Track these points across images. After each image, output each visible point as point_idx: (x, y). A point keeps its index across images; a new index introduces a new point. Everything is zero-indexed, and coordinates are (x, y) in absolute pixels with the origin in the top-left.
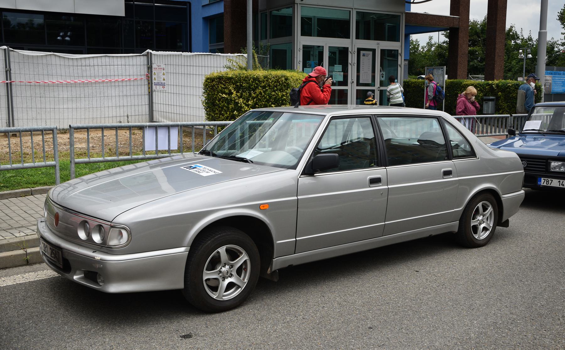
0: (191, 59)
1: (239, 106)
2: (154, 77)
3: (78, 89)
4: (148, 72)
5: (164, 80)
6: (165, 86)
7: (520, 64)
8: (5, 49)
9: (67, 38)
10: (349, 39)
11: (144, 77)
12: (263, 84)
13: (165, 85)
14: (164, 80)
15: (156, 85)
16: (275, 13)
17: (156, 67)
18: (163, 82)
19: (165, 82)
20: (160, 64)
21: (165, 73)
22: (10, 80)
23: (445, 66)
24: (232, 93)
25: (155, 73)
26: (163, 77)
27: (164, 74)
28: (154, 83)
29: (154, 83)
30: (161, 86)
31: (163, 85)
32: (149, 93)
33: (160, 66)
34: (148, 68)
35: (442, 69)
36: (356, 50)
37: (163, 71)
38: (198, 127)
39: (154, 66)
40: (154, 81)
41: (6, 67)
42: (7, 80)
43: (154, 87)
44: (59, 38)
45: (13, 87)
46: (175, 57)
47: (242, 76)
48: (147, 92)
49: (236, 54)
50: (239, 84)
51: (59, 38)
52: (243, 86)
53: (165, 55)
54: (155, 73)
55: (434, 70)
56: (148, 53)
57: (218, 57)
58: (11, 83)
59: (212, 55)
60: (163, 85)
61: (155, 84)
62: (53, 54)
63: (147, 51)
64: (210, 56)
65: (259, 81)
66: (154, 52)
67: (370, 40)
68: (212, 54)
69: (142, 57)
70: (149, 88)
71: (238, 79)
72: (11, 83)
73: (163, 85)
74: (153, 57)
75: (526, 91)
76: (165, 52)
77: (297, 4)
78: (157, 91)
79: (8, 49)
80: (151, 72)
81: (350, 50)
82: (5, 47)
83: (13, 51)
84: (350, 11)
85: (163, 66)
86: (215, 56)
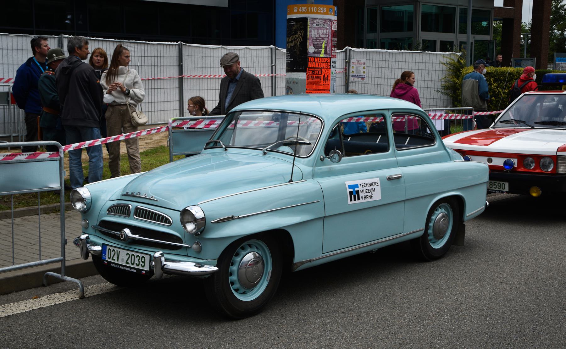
0: (384, 55)
1: (496, 94)
2: (351, 70)
3: (206, 80)
4: (346, 66)
5: (364, 72)
6: (365, 78)
7: (498, 49)
8: (271, 49)
9: (80, 22)
10: (488, 36)
11: (343, 70)
12: (516, 77)
13: (365, 77)
14: (364, 72)
15: (354, 77)
16: (386, 8)
17: (356, 61)
18: (364, 74)
19: (365, 74)
20: (359, 59)
21: (366, 67)
22: (275, 73)
23: (535, 58)
24: (492, 84)
25: (353, 66)
26: (363, 70)
27: (364, 68)
28: (352, 75)
29: (352, 75)
30: (360, 79)
31: (362, 77)
32: (346, 84)
33: (361, 61)
34: (346, 62)
35: (532, 61)
36: (459, 44)
37: (363, 66)
38: (186, 120)
39: (352, 61)
40: (351, 74)
41: (272, 63)
42: (272, 73)
43: (351, 79)
44: (67, 22)
45: (277, 79)
46: (362, 54)
47: (499, 71)
48: (344, 84)
49: (447, 53)
50: (497, 77)
51: (67, 22)
52: (500, 79)
53: (367, 52)
54: (353, 66)
55: (522, 61)
56: (346, 49)
57: (428, 56)
58: (275, 76)
59: (421, 53)
60: (363, 77)
61: (353, 76)
62: (246, 48)
63: (346, 48)
64: (422, 55)
65: (513, 75)
66: (389, 50)
67: (438, 32)
68: (422, 52)
69: (343, 53)
70: (346, 80)
71: (496, 73)
72: (275, 76)
73: (362, 77)
74: (352, 53)
75: (479, 81)
76: (367, 49)
77: (419, 2)
78: (364, 83)
79: (275, 48)
80: (349, 66)
81: (454, 43)
82: (272, 46)
83: (185, 45)
84: (455, 8)
85: (363, 61)
86: (424, 54)
